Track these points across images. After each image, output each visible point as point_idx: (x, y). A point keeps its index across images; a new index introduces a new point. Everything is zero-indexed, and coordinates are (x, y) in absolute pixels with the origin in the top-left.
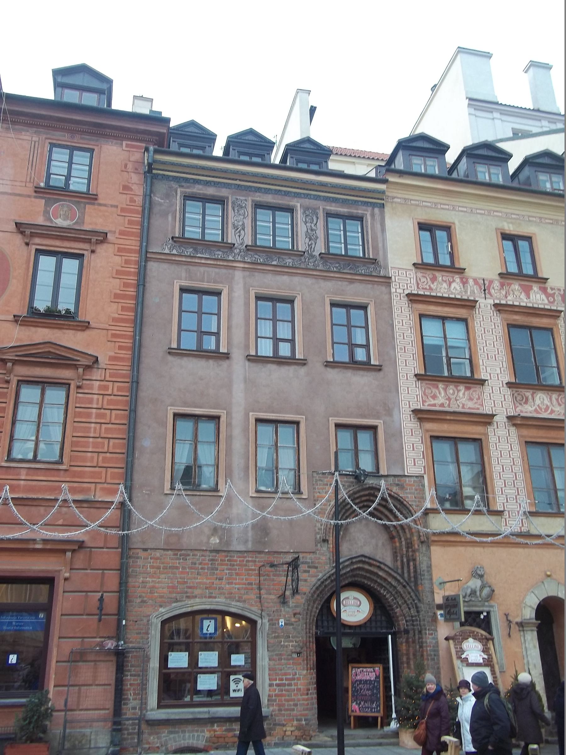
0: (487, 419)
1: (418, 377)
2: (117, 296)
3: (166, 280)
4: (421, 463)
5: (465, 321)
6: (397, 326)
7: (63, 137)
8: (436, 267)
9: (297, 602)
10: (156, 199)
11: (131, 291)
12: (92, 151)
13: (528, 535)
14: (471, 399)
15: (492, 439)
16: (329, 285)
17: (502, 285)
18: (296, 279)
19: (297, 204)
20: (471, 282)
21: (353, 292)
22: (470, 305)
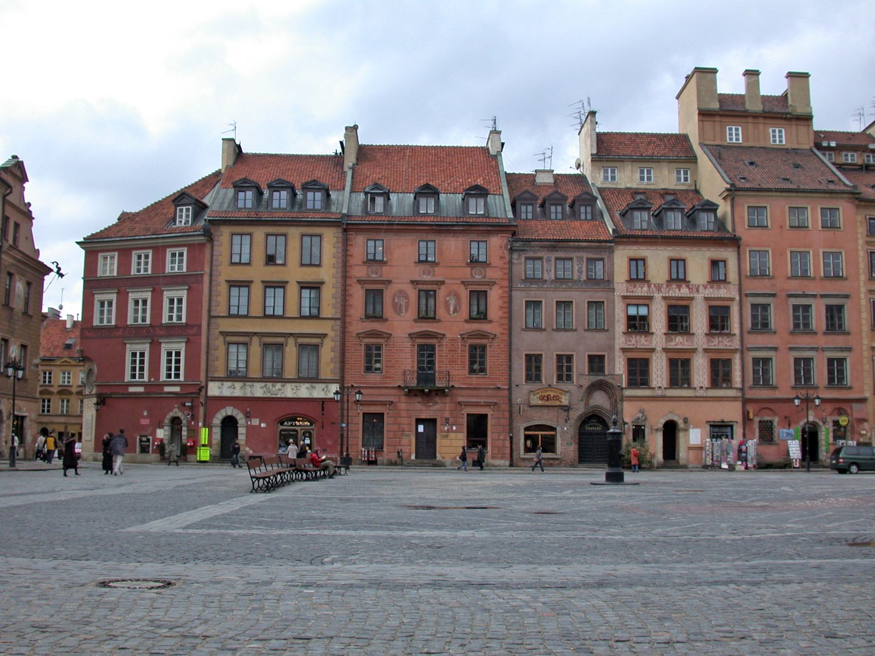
0: (652, 350)
1: (624, 333)
2: (501, 307)
3: (520, 298)
5: (648, 305)
6: (616, 311)
7: (474, 237)
8: (637, 280)
9: (572, 422)
11: (506, 305)
12: (486, 241)
13: (665, 397)
15: (654, 358)
16: (587, 294)
17: (667, 286)
18: (573, 293)
19: (574, 255)
21: (598, 296)
22: (651, 298)
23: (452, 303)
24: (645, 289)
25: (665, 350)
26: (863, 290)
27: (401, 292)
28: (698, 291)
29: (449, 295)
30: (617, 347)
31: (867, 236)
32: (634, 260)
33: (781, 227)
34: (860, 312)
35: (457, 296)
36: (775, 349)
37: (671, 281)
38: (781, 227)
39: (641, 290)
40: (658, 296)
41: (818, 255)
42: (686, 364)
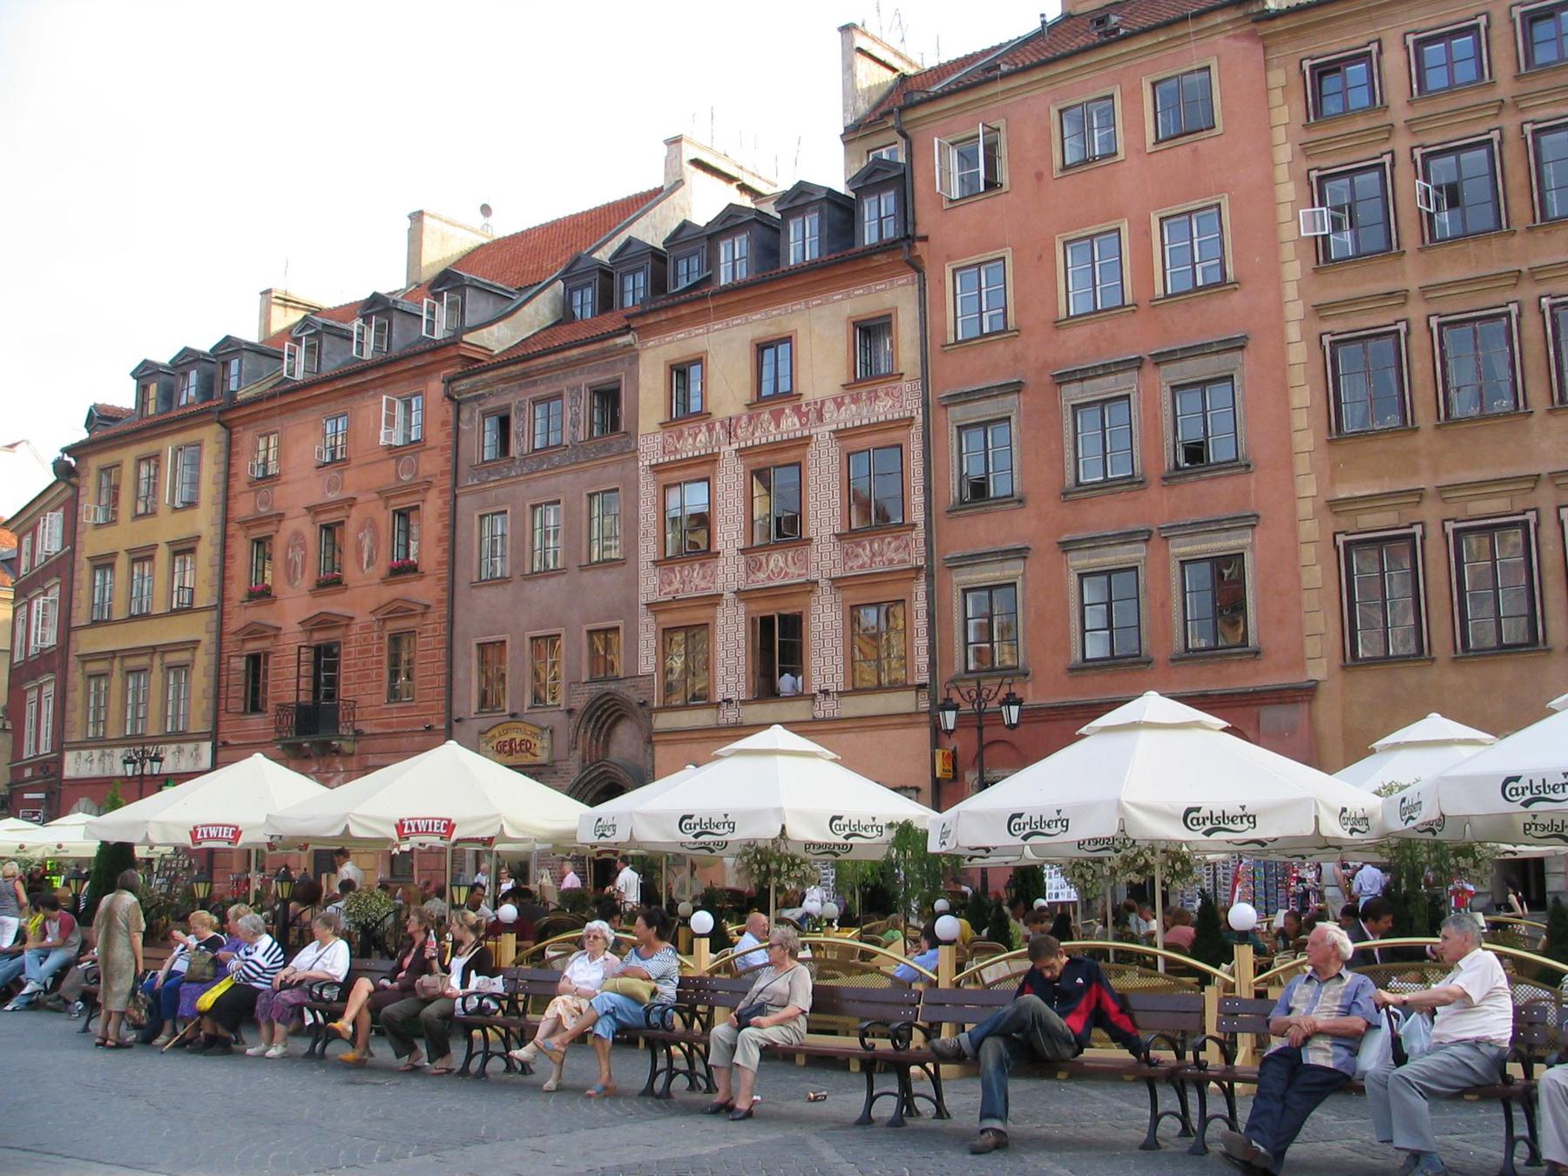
0: (714, 600)
4: (652, 660)
5: (707, 480)
10: (463, 427)
14: (704, 578)
15: (720, 621)
17: (750, 418)
18: (562, 478)
19: (563, 386)
20: (718, 425)
22: (711, 459)
23: (367, 543)
24: (702, 437)
25: (742, 595)
26: (1295, 310)
27: (297, 534)
28: (820, 417)
29: (362, 529)
30: (643, 600)
31: (1307, 127)
32: (680, 372)
33: (1039, 176)
34: (1285, 389)
35: (373, 525)
36: (1021, 553)
37: (759, 400)
38: (1039, 176)
39: (695, 443)
40: (728, 450)
41: (1148, 233)
42: (793, 625)
